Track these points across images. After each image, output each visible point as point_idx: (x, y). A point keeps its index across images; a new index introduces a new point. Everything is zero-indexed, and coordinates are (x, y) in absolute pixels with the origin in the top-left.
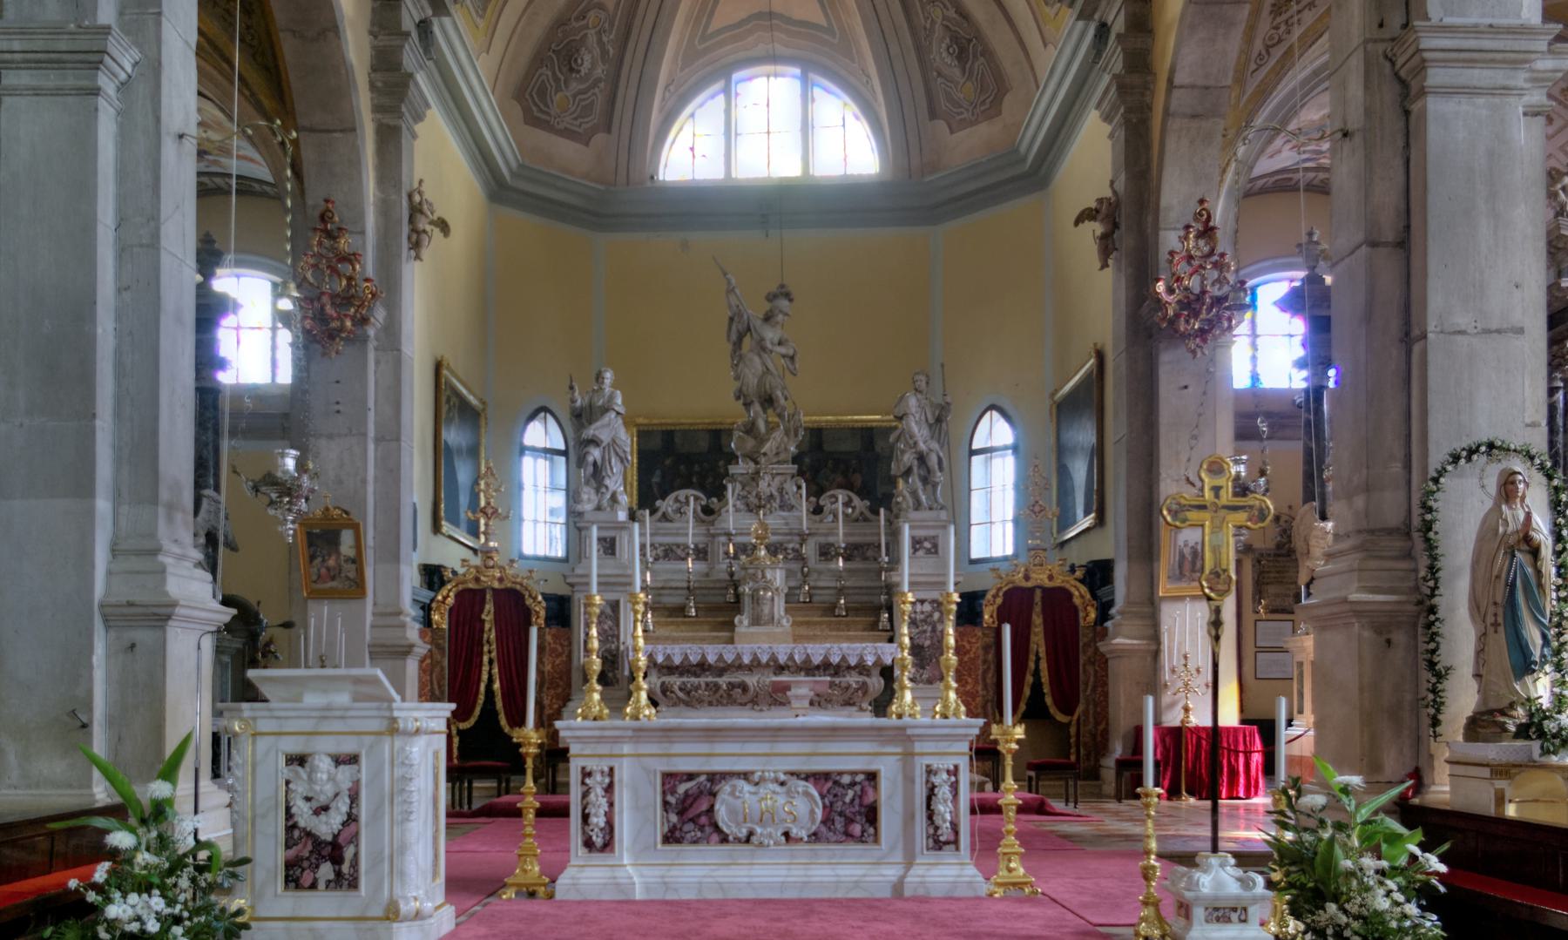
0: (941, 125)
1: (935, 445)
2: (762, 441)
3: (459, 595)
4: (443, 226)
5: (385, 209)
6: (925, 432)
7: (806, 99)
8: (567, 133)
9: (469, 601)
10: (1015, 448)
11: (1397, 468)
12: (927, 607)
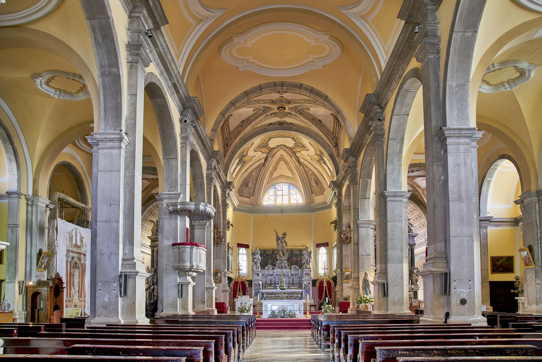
0: (314, 195)
1: (309, 259)
2: (282, 257)
3: (235, 282)
5: (224, 223)
7: (289, 189)
8: (246, 197)
9: (236, 283)
11: (357, 270)
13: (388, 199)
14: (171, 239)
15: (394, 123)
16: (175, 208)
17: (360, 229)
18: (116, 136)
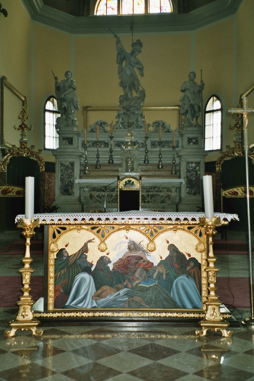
10: (221, 110)
12: (194, 165)
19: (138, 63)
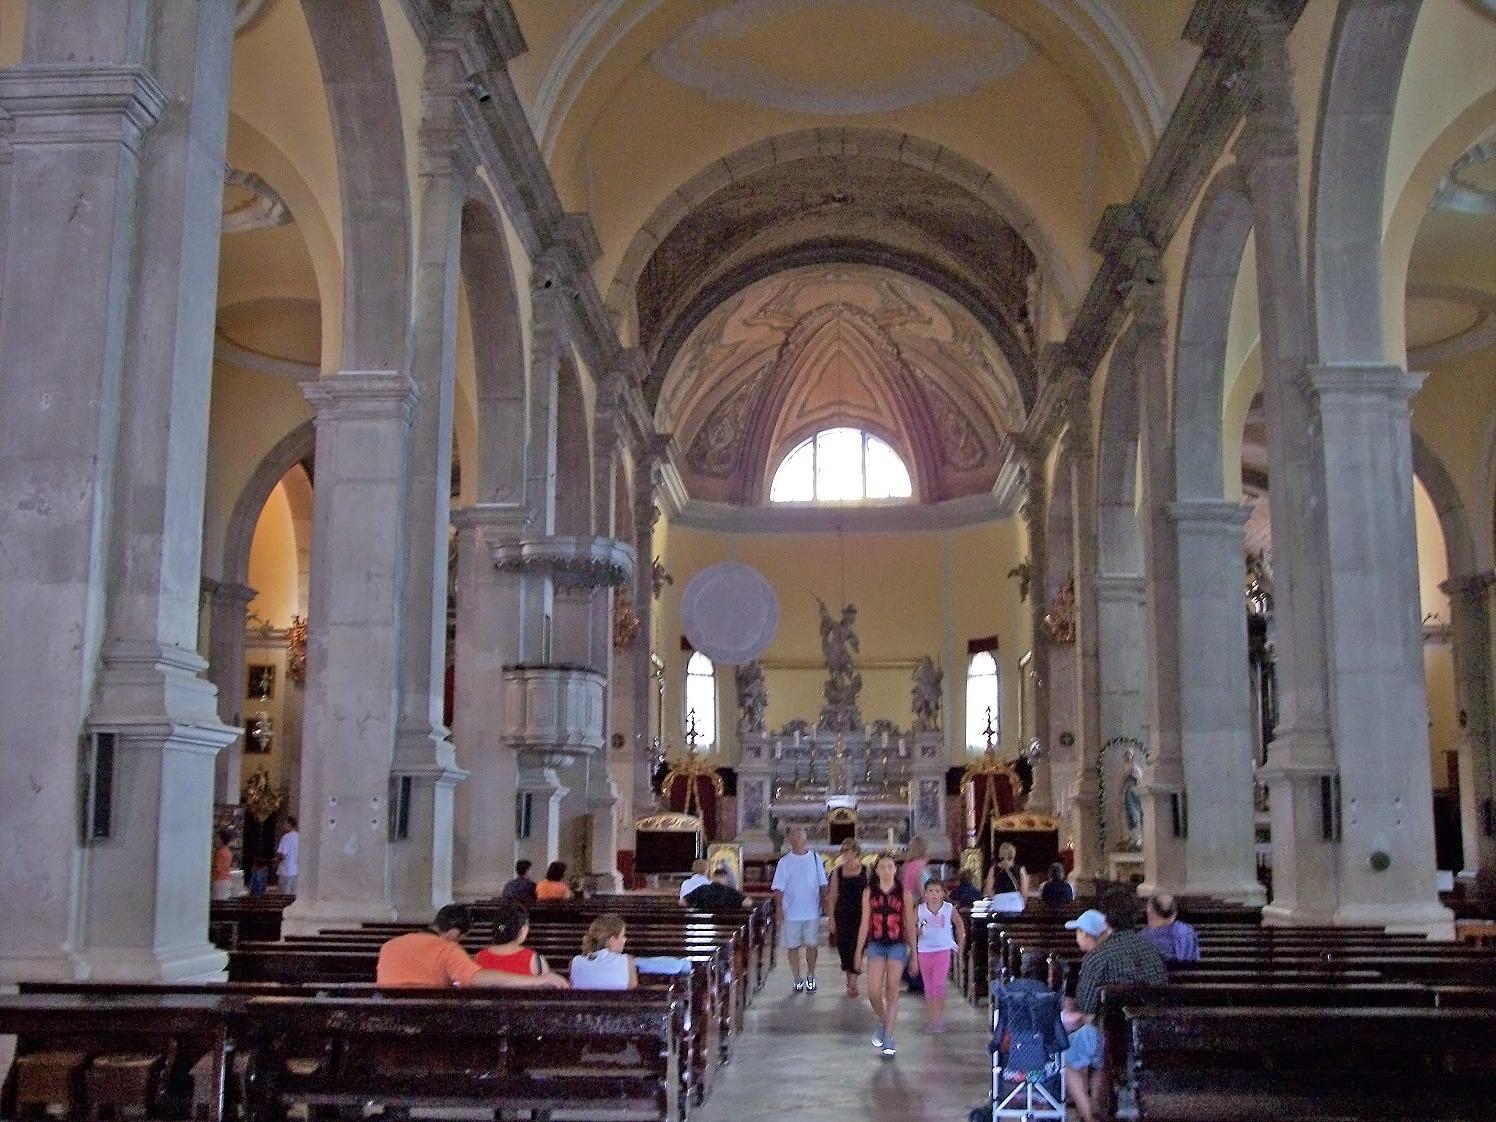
4: (669, 579)
6: (929, 689)
13: (1182, 525)
14: (497, 651)
15: (1191, 300)
16: (514, 553)
17: (1101, 604)
18: (391, 385)
19: (850, 636)
